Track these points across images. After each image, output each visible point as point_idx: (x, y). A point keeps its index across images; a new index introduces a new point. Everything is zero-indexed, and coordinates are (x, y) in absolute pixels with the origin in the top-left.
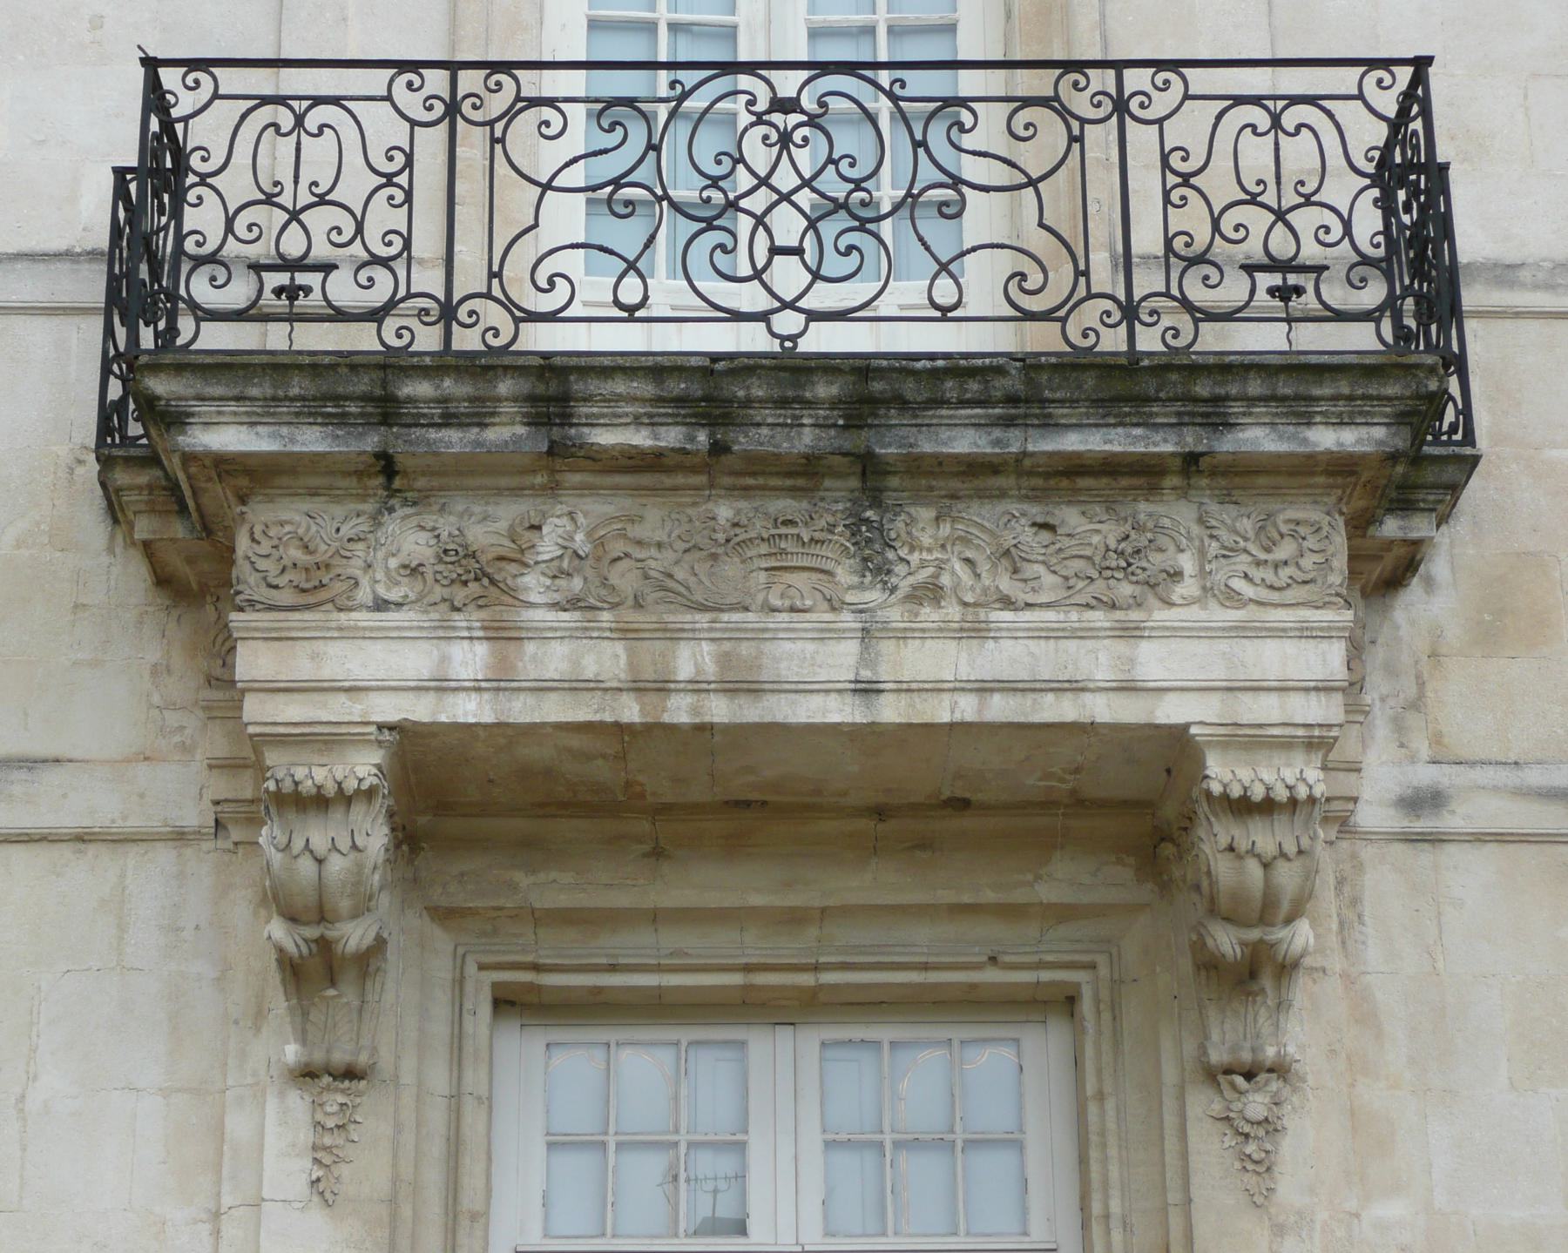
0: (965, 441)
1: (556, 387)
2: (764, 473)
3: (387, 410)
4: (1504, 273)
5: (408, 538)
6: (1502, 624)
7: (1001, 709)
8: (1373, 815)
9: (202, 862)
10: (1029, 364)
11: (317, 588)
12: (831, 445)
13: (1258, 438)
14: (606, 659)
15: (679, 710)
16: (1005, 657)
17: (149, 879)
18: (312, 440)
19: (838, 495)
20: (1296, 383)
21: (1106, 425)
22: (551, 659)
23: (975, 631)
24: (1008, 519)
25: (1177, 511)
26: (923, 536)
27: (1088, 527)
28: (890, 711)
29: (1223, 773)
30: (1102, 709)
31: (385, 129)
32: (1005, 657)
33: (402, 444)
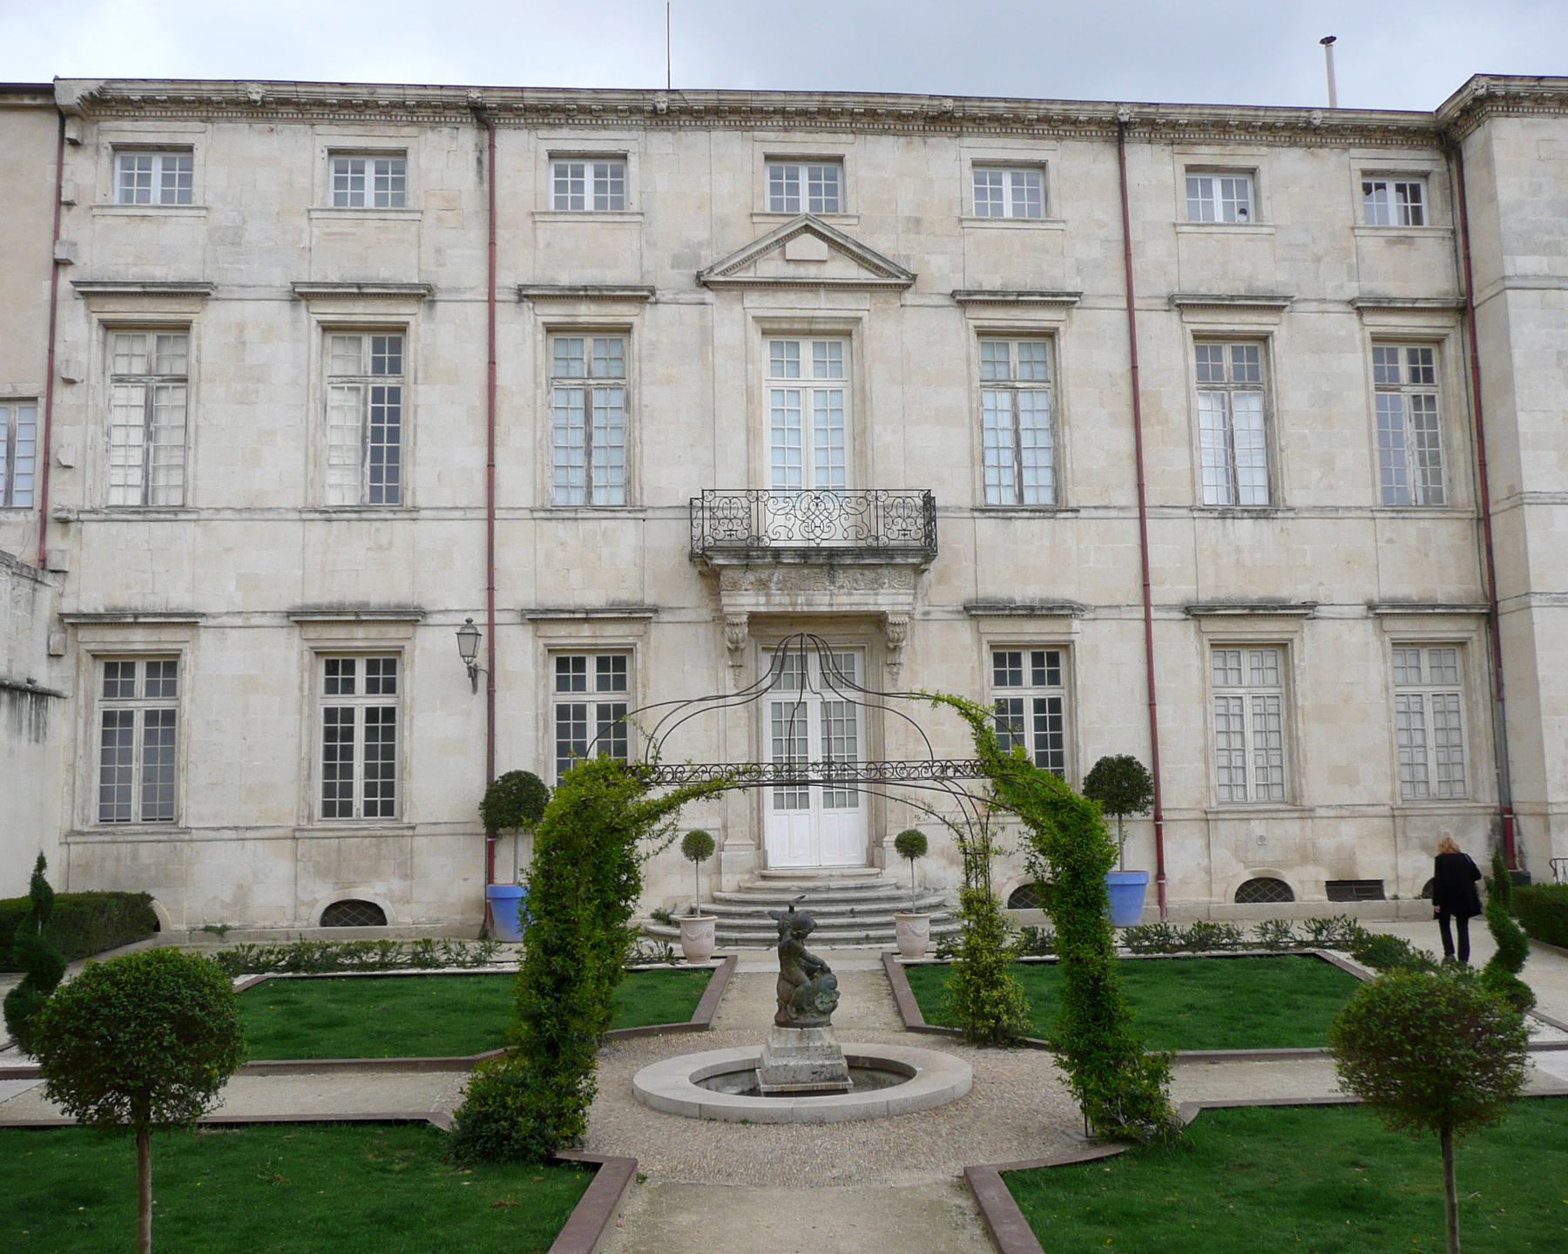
0: (849, 561)
1: (777, 553)
2: (812, 565)
3: (748, 557)
4: (946, 509)
5: (751, 577)
6: (942, 579)
7: (854, 608)
8: (917, 616)
9: (711, 626)
10: (860, 549)
11: (735, 586)
12: (822, 561)
13: (899, 560)
14: (786, 600)
15: (798, 609)
16: (856, 598)
17: (701, 629)
18: (735, 562)
19: (826, 569)
20: (906, 551)
21: (870, 558)
22: (776, 600)
23: (850, 594)
24: (856, 573)
25: (885, 572)
26: (841, 577)
27: (869, 574)
28: (835, 609)
29: (891, 619)
30: (871, 608)
31: (745, 503)
32: (856, 598)
33: (751, 562)
